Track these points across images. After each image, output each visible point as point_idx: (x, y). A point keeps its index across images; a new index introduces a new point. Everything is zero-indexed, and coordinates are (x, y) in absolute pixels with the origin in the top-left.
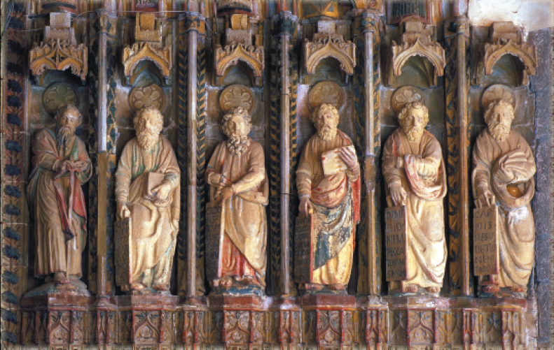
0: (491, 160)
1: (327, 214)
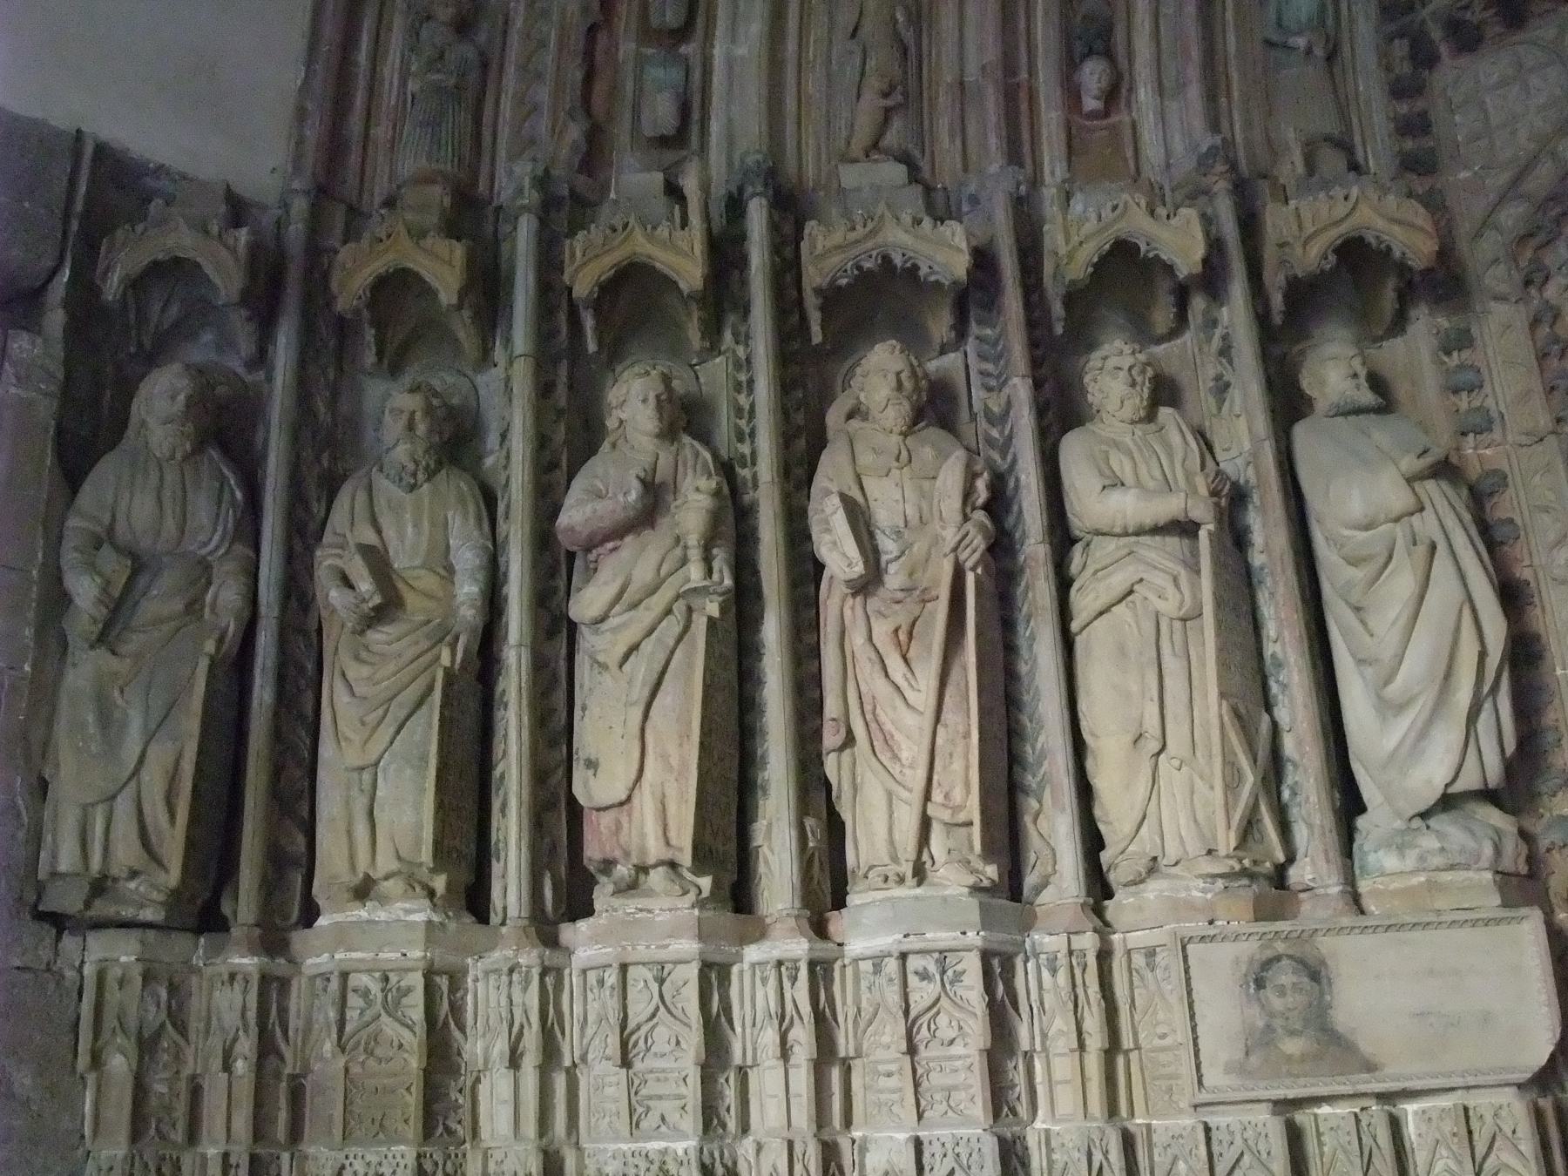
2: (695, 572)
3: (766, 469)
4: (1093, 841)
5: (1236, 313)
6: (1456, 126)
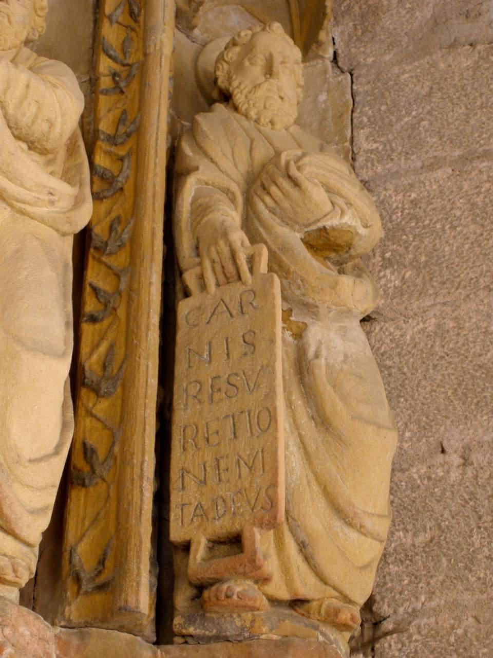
0: (243, 167)
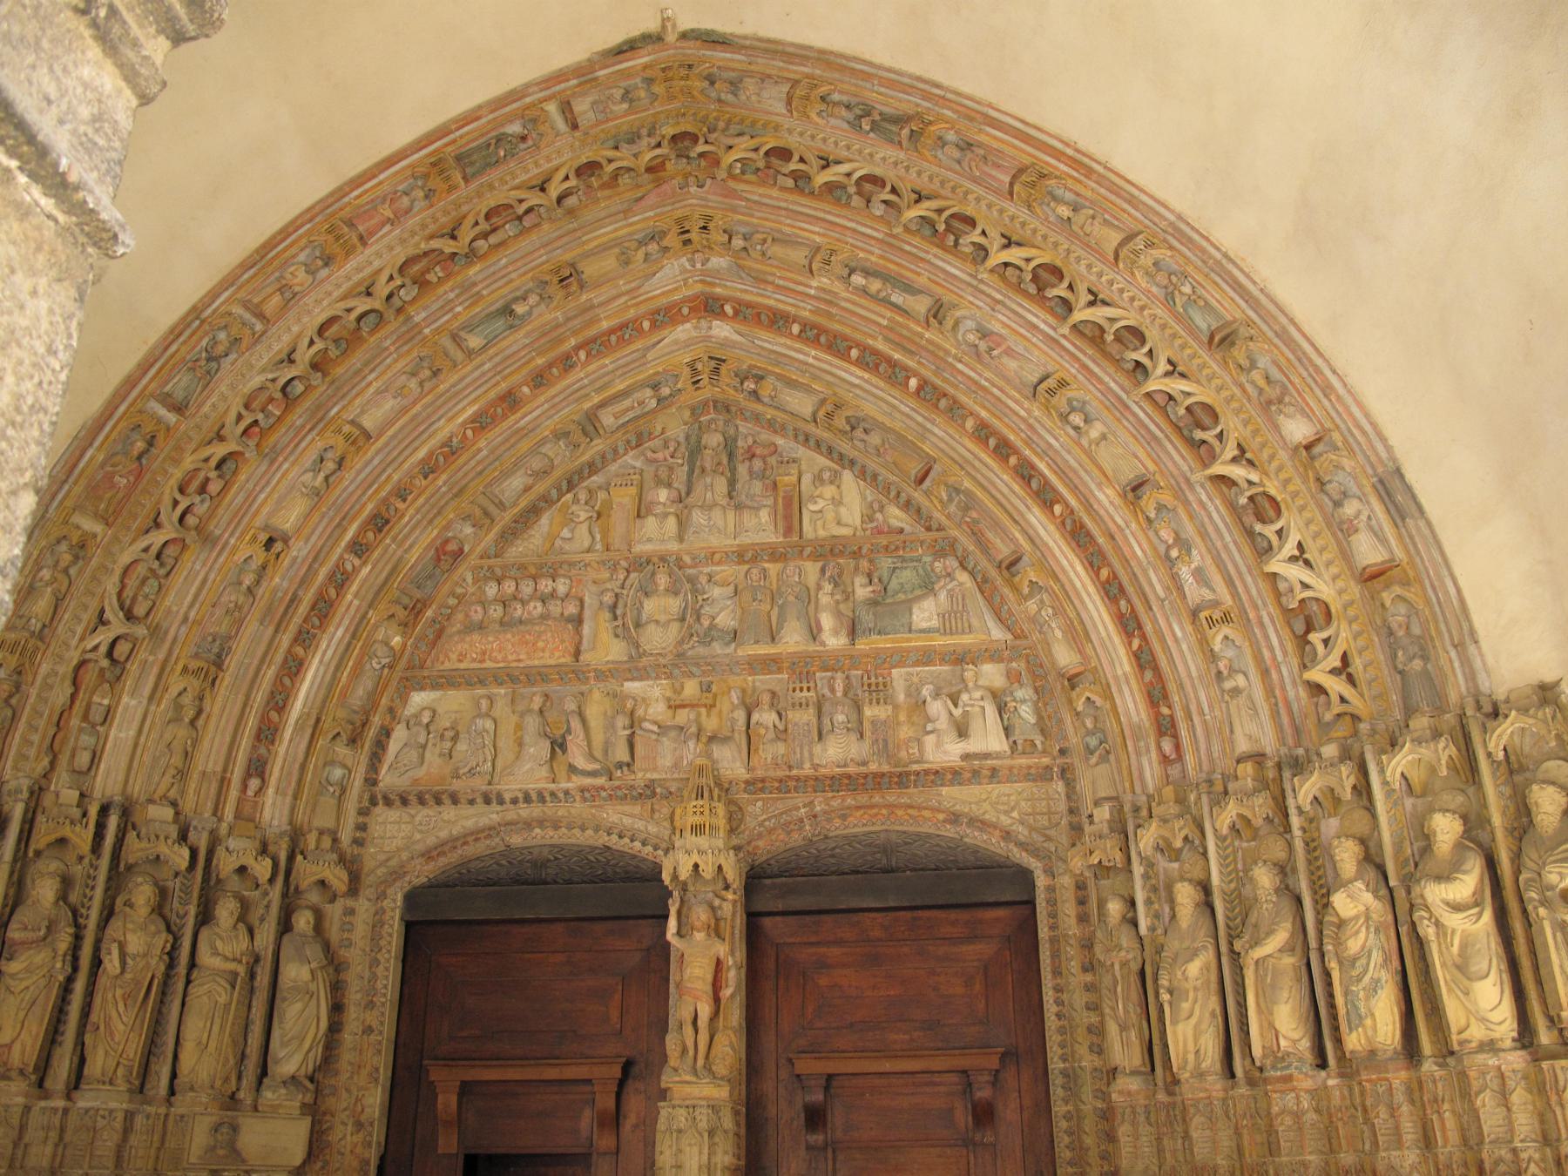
1: (1353, 966)
2: (59, 965)
3: (92, 924)
4: (174, 1076)
5: (276, 893)
6: (376, 830)
